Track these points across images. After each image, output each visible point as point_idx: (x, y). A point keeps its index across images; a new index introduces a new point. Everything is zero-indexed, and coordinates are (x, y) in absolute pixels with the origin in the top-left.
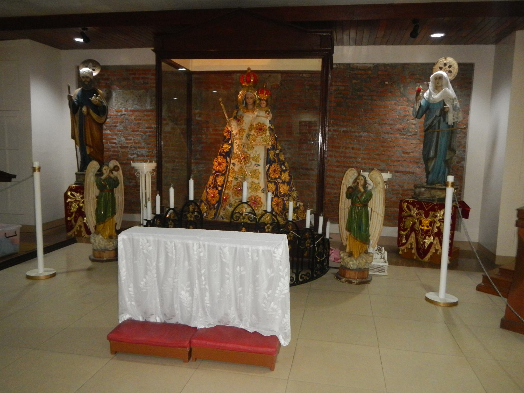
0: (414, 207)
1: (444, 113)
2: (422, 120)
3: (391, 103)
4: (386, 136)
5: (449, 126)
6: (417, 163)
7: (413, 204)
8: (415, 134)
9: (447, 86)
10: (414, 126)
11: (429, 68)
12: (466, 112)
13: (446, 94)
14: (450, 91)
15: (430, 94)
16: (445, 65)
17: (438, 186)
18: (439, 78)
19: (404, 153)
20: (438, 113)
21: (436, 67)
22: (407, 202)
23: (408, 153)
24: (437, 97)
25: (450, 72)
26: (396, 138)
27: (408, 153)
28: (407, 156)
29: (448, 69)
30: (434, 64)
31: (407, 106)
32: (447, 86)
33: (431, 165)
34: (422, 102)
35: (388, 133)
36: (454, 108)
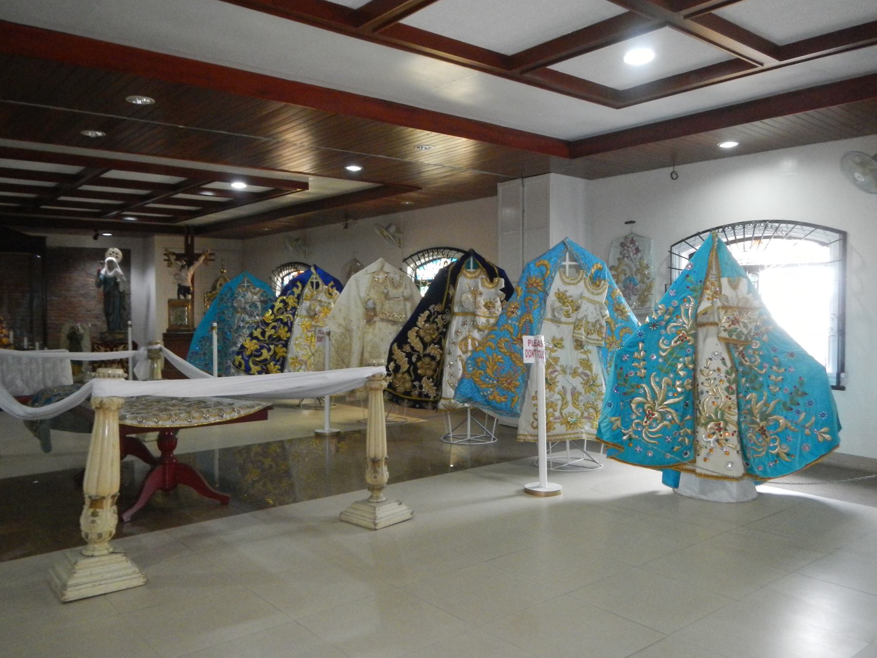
0: (102, 346)
1: (117, 284)
2: (102, 288)
3: (75, 275)
4: (72, 300)
5: (120, 293)
6: (97, 318)
7: (102, 345)
8: (95, 297)
9: (117, 267)
10: (92, 292)
11: (100, 254)
12: (129, 282)
13: (116, 272)
14: (119, 270)
15: (106, 272)
16: (113, 252)
17: (117, 331)
18: (111, 262)
19: (88, 311)
20: (112, 284)
21: (108, 253)
22: (97, 344)
23: (90, 311)
24: (111, 274)
25: (117, 257)
26: (80, 301)
27: (90, 311)
28: (89, 313)
29: (116, 255)
30: (105, 250)
31: (87, 277)
32: (117, 267)
33: (111, 319)
34: (101, 277)
35: (74, 297)
36: (123, 281)
